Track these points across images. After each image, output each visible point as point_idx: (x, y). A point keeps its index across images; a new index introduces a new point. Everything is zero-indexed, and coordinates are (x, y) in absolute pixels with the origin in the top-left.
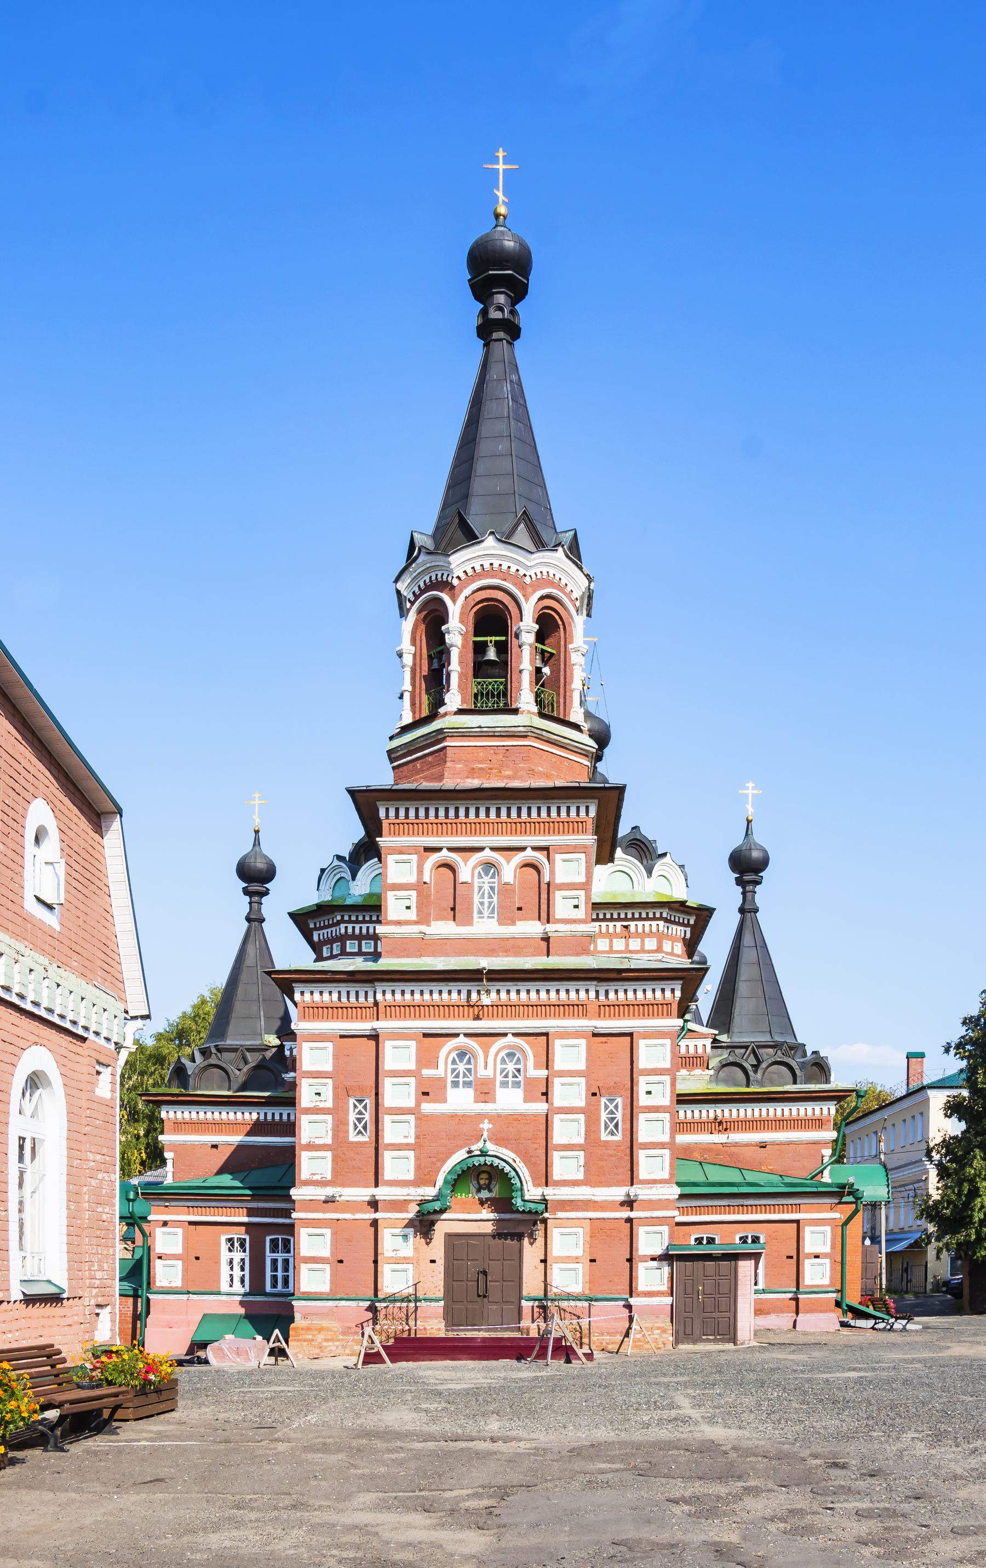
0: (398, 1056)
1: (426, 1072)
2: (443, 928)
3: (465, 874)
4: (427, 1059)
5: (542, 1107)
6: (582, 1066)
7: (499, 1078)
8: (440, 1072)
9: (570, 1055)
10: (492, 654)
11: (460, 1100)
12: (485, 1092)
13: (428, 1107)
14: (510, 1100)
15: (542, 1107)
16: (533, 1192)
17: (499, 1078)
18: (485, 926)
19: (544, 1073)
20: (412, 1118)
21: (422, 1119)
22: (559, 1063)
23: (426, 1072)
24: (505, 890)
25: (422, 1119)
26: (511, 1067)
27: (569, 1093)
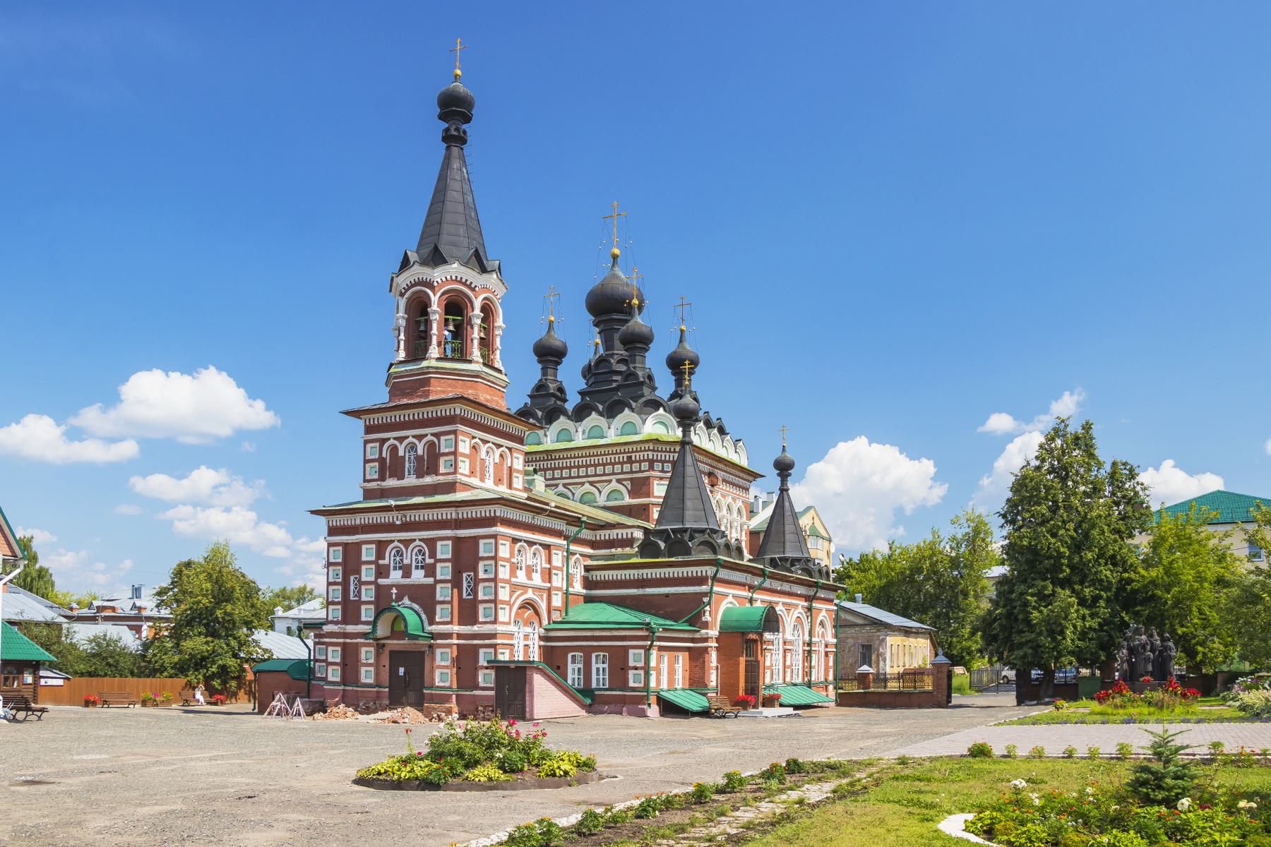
0: (368, 553)
1: (381, 562)
2: (391, 483)
3: (401, 453)
4: (380, 555)
5: (430, 580)
6: (449, 556)
7: (414, 564)
8: (386, 562)
9: (445, 550)
10: (422, 328)
11: (396, 576)
12: (407, 572)
13: (381, 581)
14: (418, 576)
15: (430, 580)
16: (429, 628)
17: (414, 564)
18: (410, 481)
19: (432, 561)
20: (373, 587)
21: (379, 588)
22: (439, 556)
23: (381, 562)
24: (419, 459)
25: (378, 587)
26: (420, 558)
27: (444, 571)
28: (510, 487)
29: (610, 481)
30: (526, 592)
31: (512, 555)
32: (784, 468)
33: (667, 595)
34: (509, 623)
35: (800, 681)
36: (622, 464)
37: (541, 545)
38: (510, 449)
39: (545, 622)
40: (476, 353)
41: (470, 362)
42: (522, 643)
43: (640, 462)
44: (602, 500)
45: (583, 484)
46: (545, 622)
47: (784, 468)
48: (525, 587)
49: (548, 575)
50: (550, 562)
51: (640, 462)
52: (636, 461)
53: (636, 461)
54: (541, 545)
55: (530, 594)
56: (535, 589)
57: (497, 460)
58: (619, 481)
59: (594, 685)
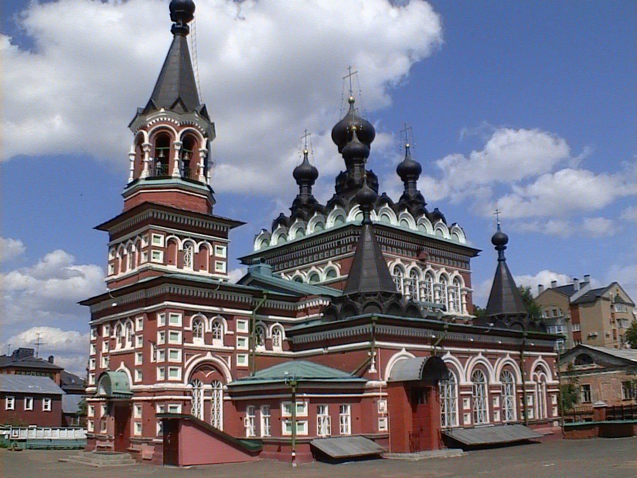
28: (212, 271)
29: (327, 263)
30: (205, 355)
31: (185, 323)
32: (500, 242)
33: (343, 352)
34: (182, 382)
35: (515, 419)
36: (334, 248)
37: (221, 315)
38: (211, 242)
39: (229, 380)
40: (176, 172)
41: (171, 178)
42: (202, 398)
43: (346, 245)
44: (323, 278)
45: (310, 267)
46: (229, 380)
47: (500, 242)
48: (203, 351)
49: (229, 340)
50: (232, 327)
51: (346, 245)
52: (343, 245)
53: (343, 245)
54: (221, 315)
55: (209, 356)
56: (214, 352)
57: (197, 250)
58: (333, 262)
59: (263, 434)
